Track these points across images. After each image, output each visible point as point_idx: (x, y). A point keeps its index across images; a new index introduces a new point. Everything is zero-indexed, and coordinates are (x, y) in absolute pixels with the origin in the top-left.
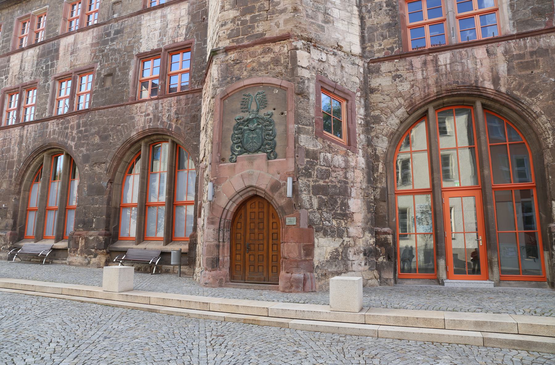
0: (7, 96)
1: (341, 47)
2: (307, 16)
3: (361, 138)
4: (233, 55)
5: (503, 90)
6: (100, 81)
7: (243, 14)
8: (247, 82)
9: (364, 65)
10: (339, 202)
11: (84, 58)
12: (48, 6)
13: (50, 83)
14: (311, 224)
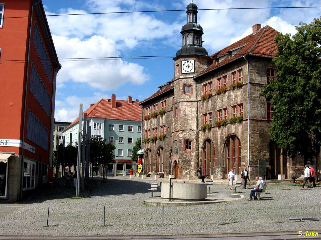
0: (153, 131)
2: (183, 125)
11: (164, 122)
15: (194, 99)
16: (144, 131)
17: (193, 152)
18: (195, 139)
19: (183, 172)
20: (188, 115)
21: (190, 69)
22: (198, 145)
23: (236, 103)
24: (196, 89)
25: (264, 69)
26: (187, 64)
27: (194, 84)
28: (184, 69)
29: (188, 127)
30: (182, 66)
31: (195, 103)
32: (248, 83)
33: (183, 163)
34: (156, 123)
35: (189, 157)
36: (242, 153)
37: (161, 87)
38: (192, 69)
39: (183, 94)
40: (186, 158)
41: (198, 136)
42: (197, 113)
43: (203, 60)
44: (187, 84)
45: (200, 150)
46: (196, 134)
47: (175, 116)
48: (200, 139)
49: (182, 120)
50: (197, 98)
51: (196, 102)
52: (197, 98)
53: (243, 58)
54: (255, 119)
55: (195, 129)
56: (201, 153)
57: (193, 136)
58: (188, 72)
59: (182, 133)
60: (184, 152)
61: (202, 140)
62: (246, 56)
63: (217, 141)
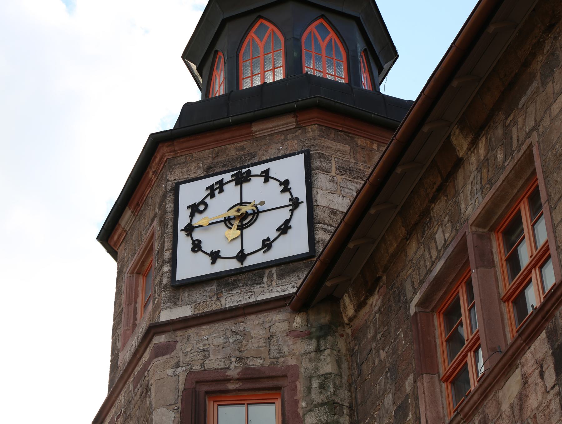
21: (266, 226)
26: (222, 205)
30: (184, 220)
38: (284, 228)
58: (241, 256)
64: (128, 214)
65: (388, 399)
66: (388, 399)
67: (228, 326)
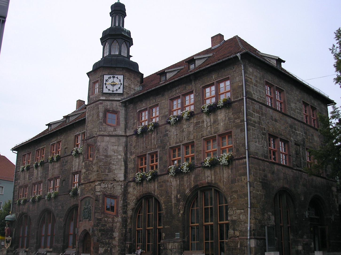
1: (116, 180)
2: (102, 172)
3: (120, 211)
4: (83, 186)
5: (156, 194)
6: (61, 183)
7: (86, 171)
8: (86, 196)
9: (124, 184)
10: (109, 234)
11: (56, 172)
12: (45, 146)
13: (47, 182)
14: (98, 241)
15: (120, 131)
16: (18, 187)
17: (117, 216)
18: (121, 196)
19: (100, 249)
20: (110, 156)
22: (125, 206)
23: (215, 133)
24: (126, 119)
25: (262, 82)
27: (122, 112)
28: (106, 87)
29: (111, 176)
30: (104, 83)
31: (124, 139)
32: (244, 98)
33: (100, 234)
34: (40, 175)
35: (111, 224)
36: (231, 215)
37: (49, 125)
38: (119, 88)
39: (104, 124)
40: (105, 225)
41: (127, 190)
42: (126, 154)
43: (134, 78)
44: (111, 110)
45: (130, 213)
46: (123, 187)
47: (88, 158)
48: (129, 196)
49: (101, 164)
50: (126, 132)
51: (124, 138)
52: (126, 132)
53: (237, 57)
54: (256, 157)
55: (122, 179)
56: (131, 218)
57: (119, 191)
58: (113, 91)
59: (100, 185)
60: (103, 216)
61: (134, 197)
62: (241, 55)
63: (170, 197)
64: (93, 73)
65: (132, 121)
66: (132, 121)
67: (111, 102)
